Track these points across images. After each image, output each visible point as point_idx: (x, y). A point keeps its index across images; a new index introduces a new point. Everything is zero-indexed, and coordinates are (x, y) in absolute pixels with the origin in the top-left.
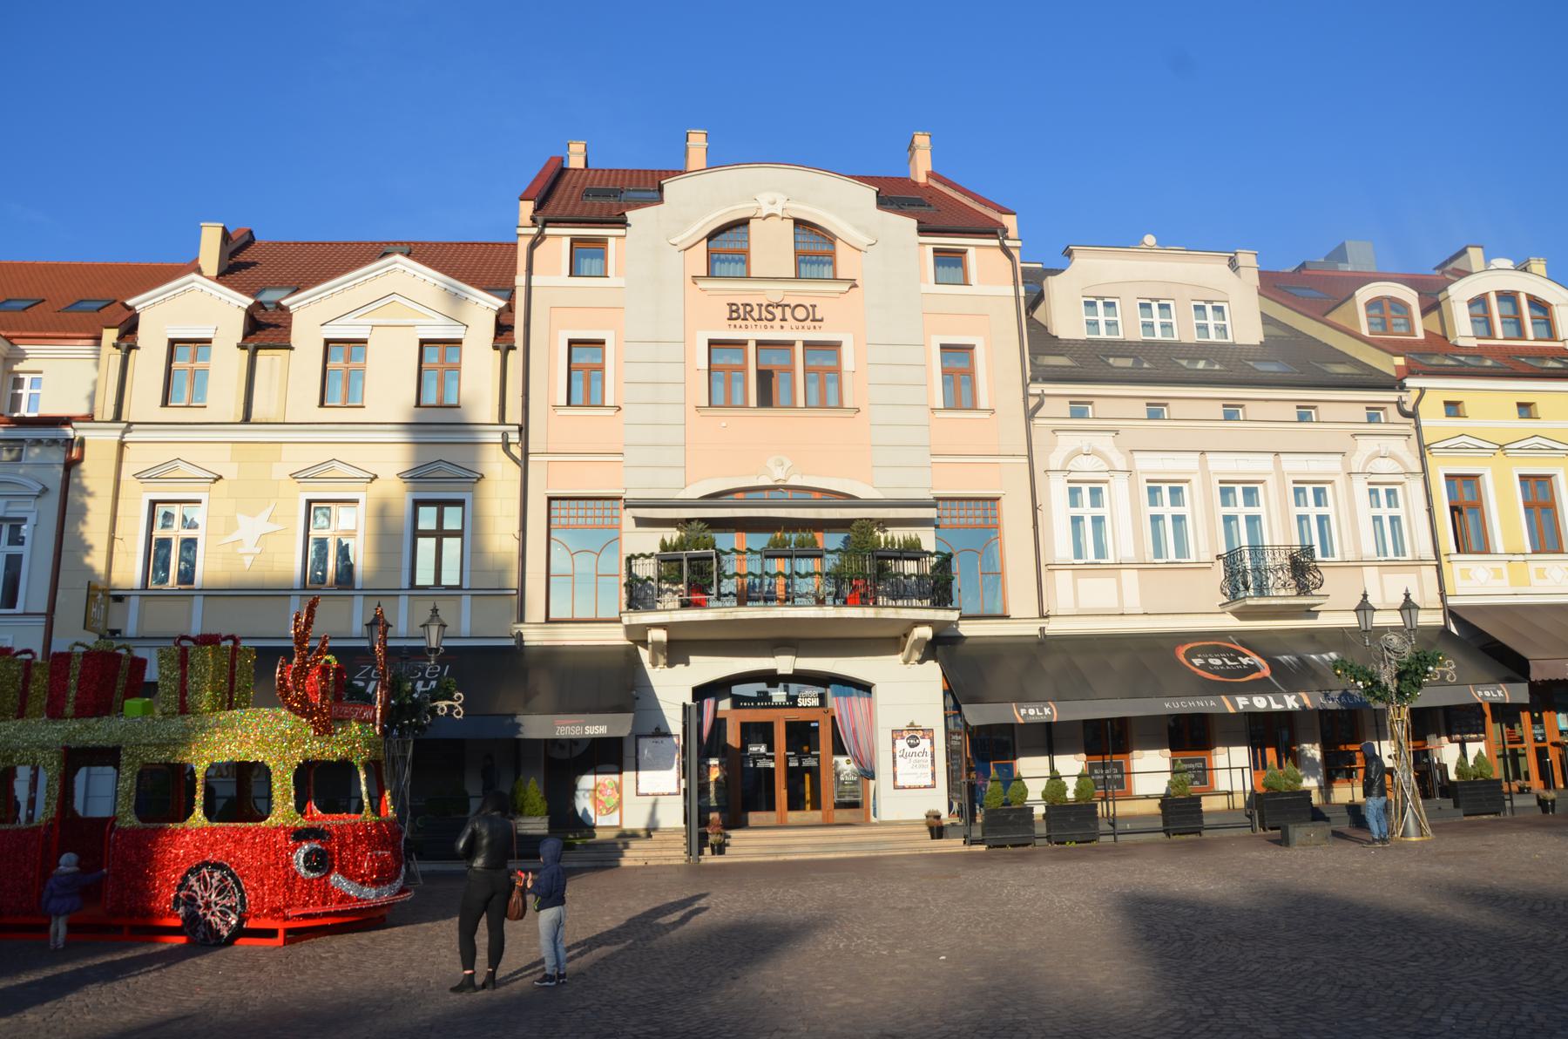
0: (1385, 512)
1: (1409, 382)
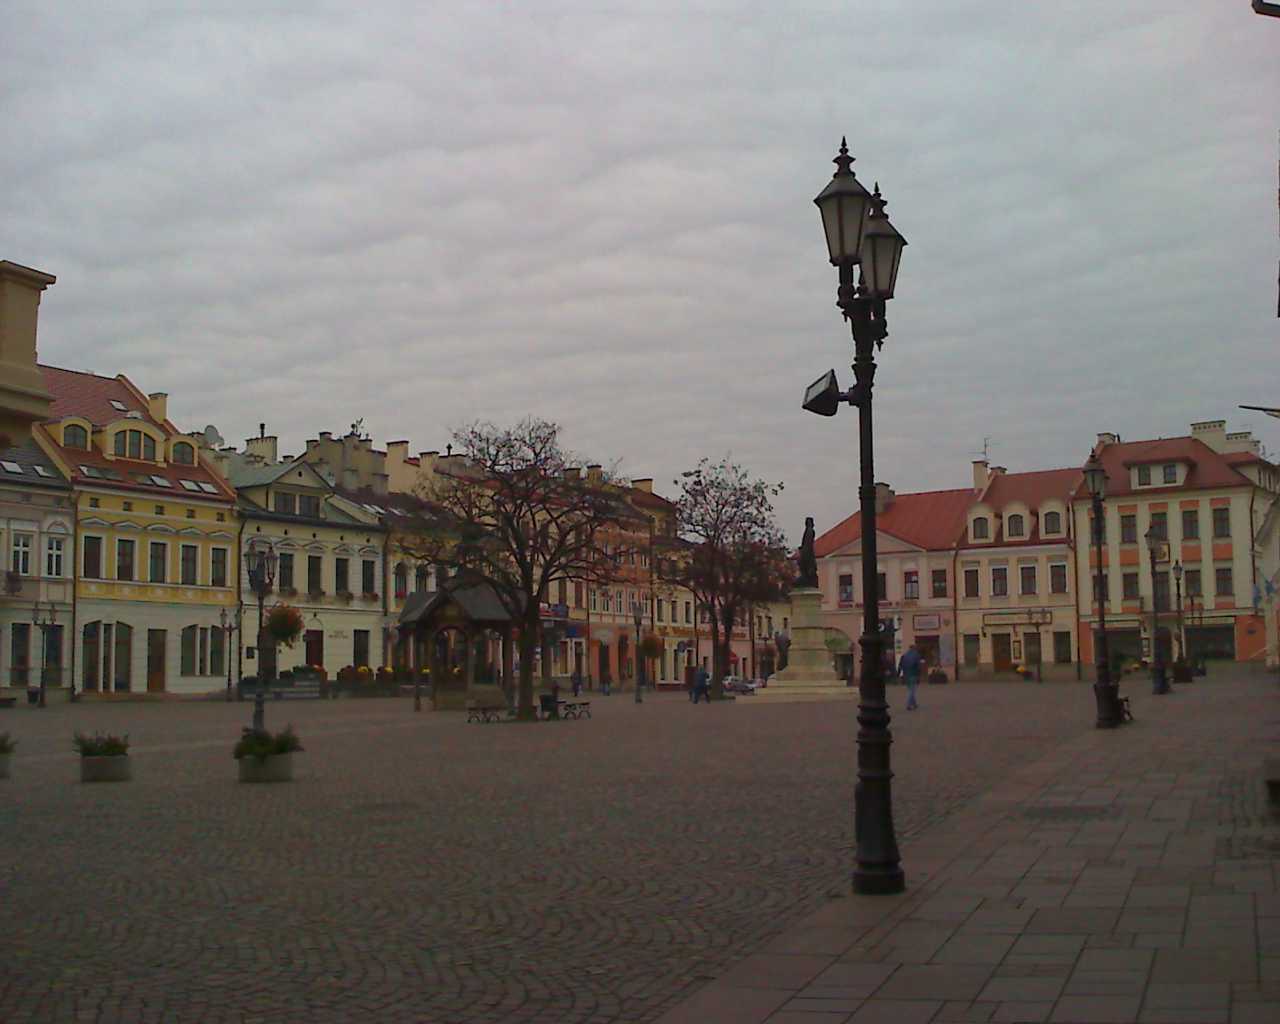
0: (55, 552)
1: (76, 488)
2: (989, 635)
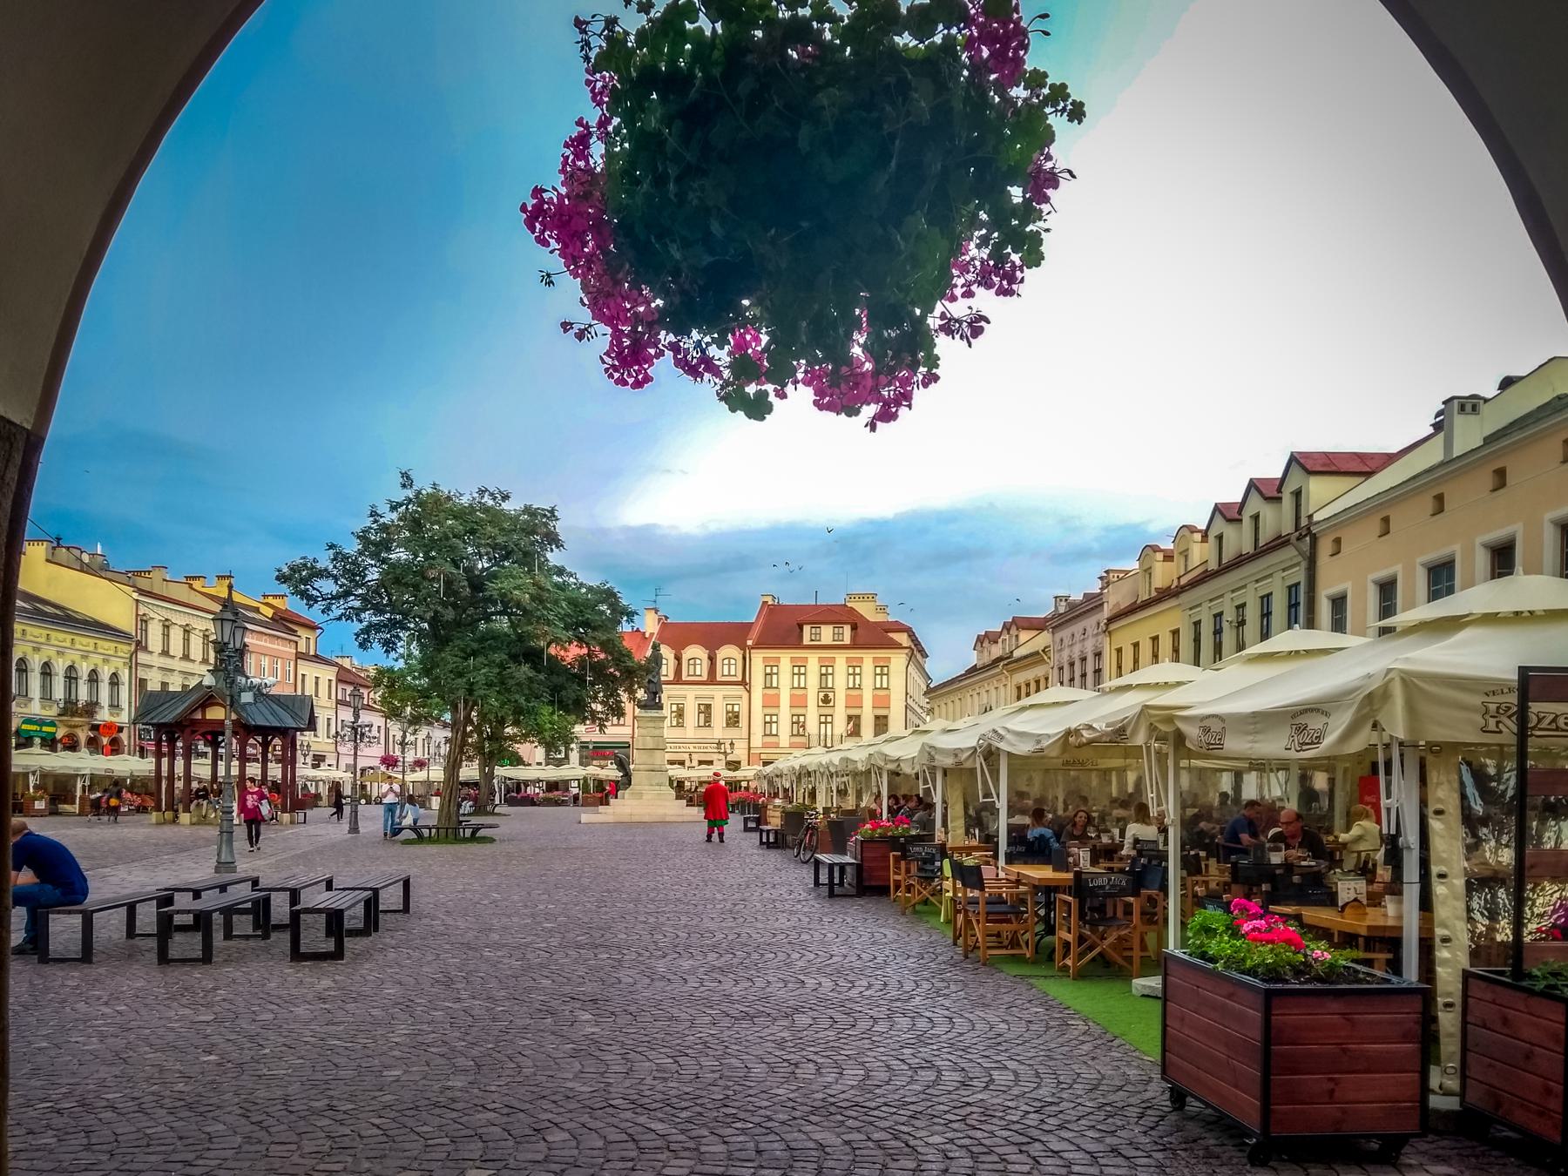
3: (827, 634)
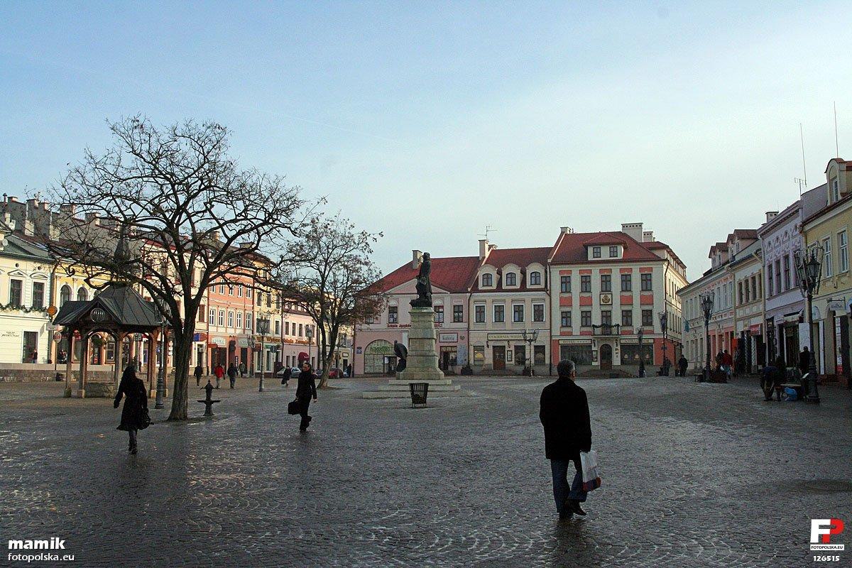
2: (491, 348)
3: (605, 253)
